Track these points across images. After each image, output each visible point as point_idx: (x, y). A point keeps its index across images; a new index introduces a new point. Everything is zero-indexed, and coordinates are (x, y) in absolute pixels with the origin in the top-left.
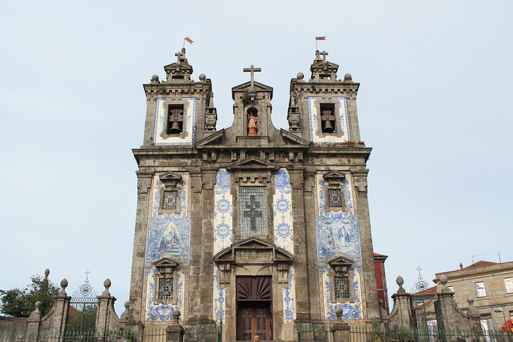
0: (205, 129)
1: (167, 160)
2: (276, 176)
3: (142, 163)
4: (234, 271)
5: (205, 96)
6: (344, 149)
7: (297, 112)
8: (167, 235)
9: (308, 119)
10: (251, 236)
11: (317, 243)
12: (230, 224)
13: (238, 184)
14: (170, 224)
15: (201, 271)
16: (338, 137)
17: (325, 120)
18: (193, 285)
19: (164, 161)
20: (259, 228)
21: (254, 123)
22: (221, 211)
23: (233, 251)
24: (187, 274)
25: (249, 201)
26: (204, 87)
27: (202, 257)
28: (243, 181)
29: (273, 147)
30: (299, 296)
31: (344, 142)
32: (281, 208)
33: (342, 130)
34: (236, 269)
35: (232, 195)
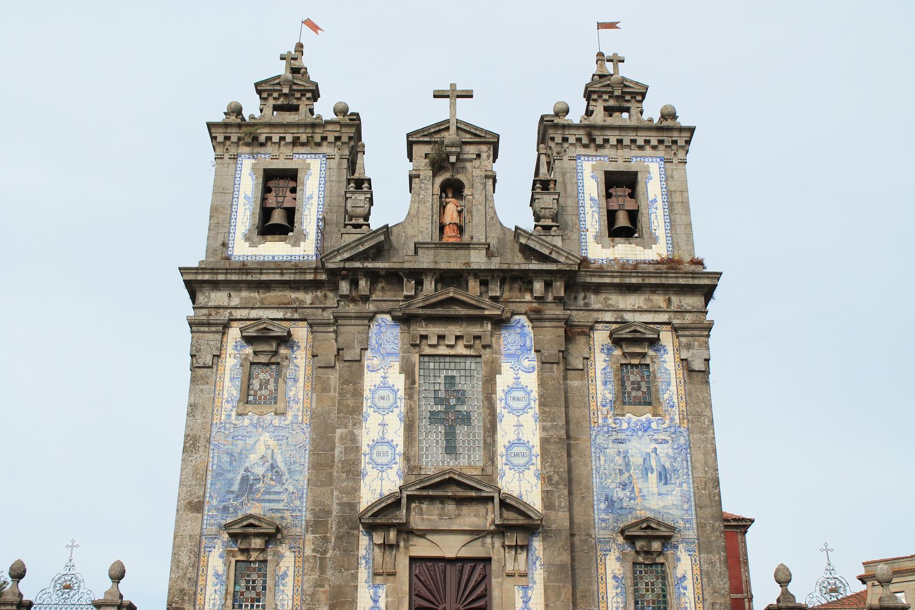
0: (346, 225)
1: (258, 292)
2: (504, 333)
3: (201, 299)
4: (407, 548)
5: (346, 152)
6: (657, 274)
7: (552, 191)
8: (255, 463)
9: (578, 206)
10: (446, 467)
11: (595, 485)
12: (399, 439)
13: (417, 349)
14: (262, 438)
15: (330, 546)
16: (645, 248)
17: (616, 208)
19: (252, 295)
20: (464, 450)
21: (456, 214)
22: (377, 409)
23: (404, 501)
24: (299, 552)
25: (442, 388)
26: (344, 130)
27: (334, 513)
28: (429, 343)
29: (497, 267)
30: (552, 605)
31: (656, 258)
33: (653, 231)
34: (411, 543)
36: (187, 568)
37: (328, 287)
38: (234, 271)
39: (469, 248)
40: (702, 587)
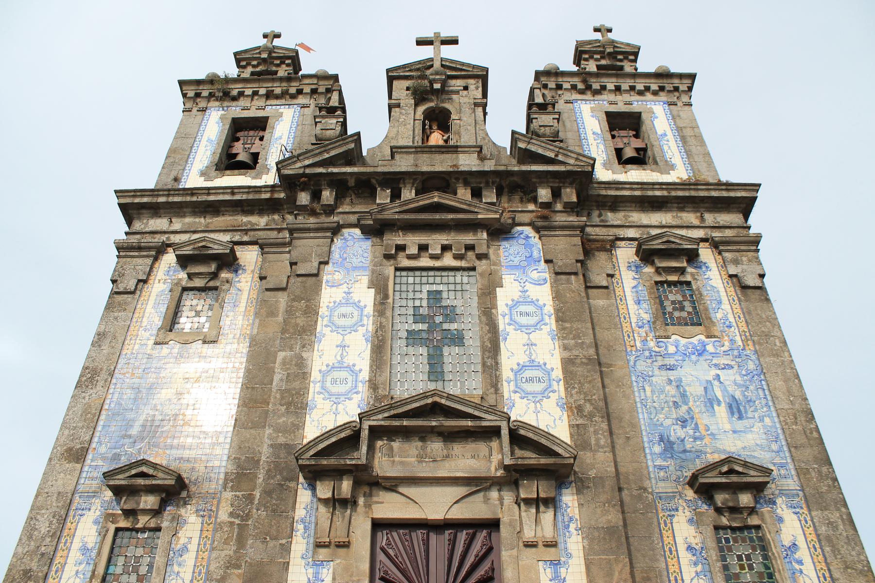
1: (205, 217)
2: (505, 244)
4: (368, 506)
13: (392, 262)
17: (622, 146)
18: (223, 554)
19: (197, 220)
22: (335, 328)
23: (365, 434)
24: (210, 517)
25: (425, 303)
26: (321, 83)
27: (263, 458)
29: (492, 169)
32: (524, 320)
33: (669, 159)
34: (375, 499)
35: (373, 290)
36: (43, 538)
37: (288, 208)
38: (177, 192)
39: (457, 152)
40: (826, 559)
